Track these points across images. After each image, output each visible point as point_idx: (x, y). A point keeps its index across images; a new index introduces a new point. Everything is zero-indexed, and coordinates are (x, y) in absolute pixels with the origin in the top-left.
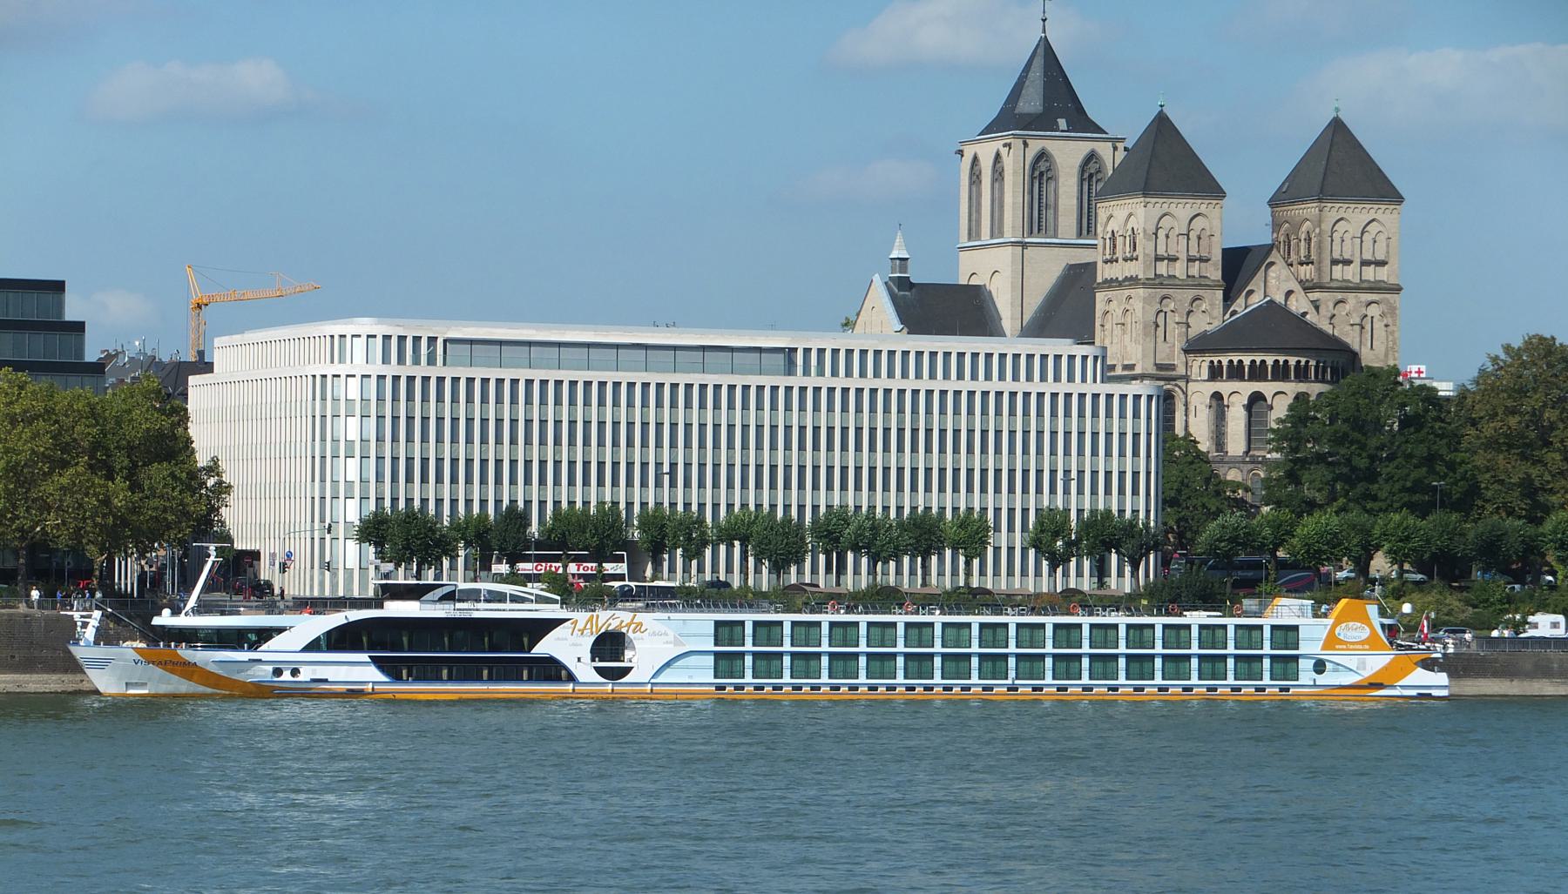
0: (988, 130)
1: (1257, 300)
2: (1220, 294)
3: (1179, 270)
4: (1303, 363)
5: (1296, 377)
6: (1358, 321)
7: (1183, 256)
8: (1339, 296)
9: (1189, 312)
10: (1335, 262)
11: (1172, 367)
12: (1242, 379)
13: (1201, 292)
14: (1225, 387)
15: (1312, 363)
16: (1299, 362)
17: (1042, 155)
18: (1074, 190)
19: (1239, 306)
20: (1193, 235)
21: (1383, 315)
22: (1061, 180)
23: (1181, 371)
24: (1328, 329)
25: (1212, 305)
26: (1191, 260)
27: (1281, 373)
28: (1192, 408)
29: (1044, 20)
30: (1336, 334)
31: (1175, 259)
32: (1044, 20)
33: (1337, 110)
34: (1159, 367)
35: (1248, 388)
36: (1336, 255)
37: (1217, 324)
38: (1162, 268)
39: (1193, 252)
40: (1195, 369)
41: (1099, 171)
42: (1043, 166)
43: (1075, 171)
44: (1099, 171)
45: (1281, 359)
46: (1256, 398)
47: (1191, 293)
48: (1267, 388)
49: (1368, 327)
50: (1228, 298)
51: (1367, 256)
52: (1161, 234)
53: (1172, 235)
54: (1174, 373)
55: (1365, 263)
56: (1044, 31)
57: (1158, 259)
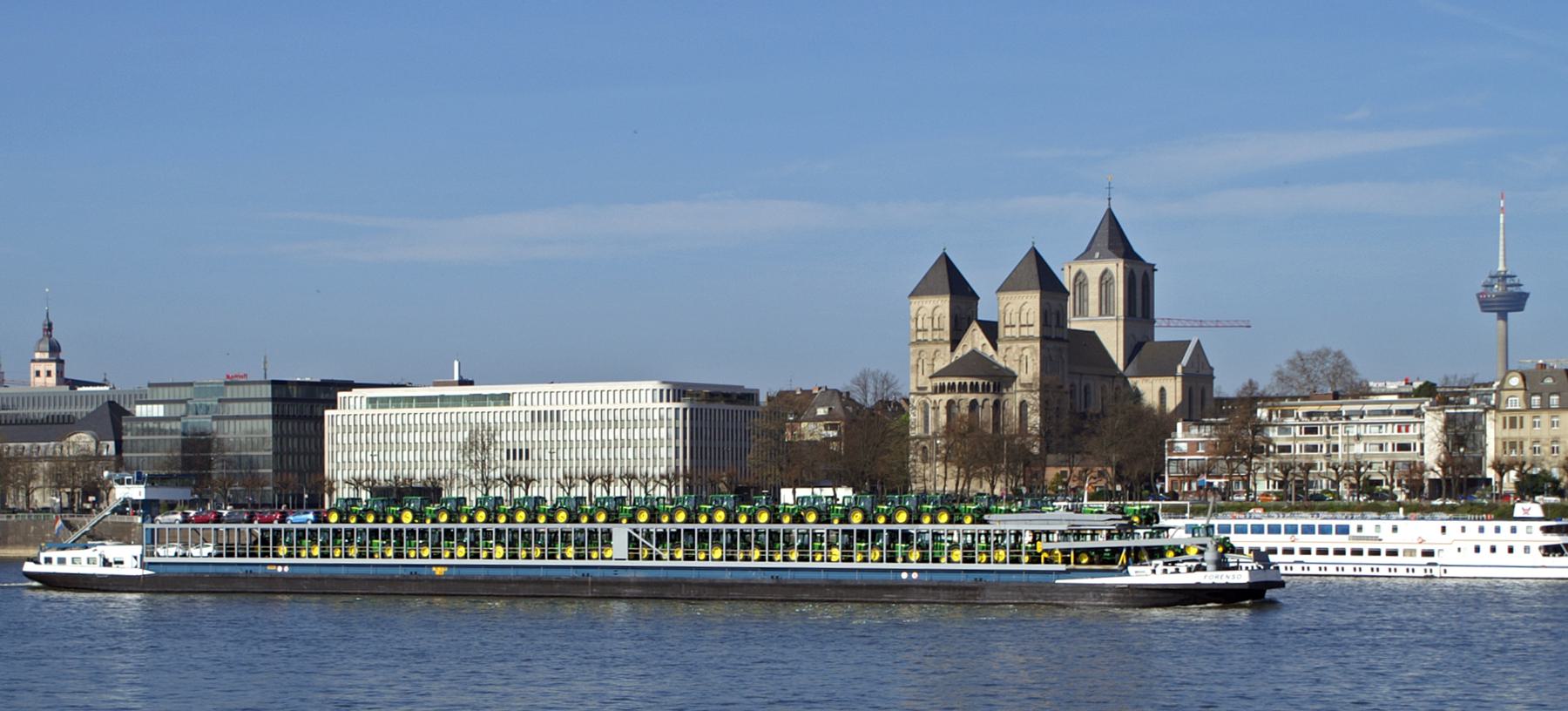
0: (1077, 259)
1: (969, 349)
2: (948, 347)
3: (929, 337)
4: (986, 383)
5: (994, 390)
6: (1017, 358)
7: (930, 329)
8: (1008, 345)
9: (933, 359)
10: (1006, 326)
11: (925, 388)
12: (966, 392)
13: (939, 347)
15: (991, 384)
16: (984, 383)
17: (1079, 273)
18: (1097, 291)
19: (959, 353)
21: (1031, 353)
22: (1090, 286)
24: (1002, 363)
25: (945, 354)
26: (934, 330)
27: (963, 388)
29: (1109, 199)
30: (1008, 366)
31: (926, 330)
32: (1109, 199)
33: (1033, 243)
34: (919, 388)
35: (946, 397)
36: (1008, 323)
37: (947, 364)
38: (920, 336)
39: (936, 326)
41: (1110, 279)
42: (1081, 278)
43: (1097, 280)
44: (1110, 279)
45: (974, 381)
46: (950, 404)
47: (934, 347)
48: (980, 398)
49: (1025, 362)
50: (953, 350)
51: (1024, 322)
52: (920, 319)
53: (925, 318)
54: (926, 392)
55: (1022, 326)
56: (1109, 204)
57: (918, 330)
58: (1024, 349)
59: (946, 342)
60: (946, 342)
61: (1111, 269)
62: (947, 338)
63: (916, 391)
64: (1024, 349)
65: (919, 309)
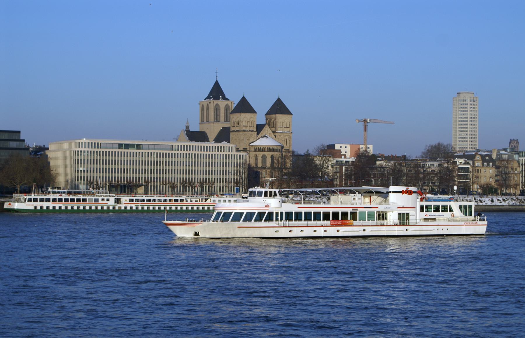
2: (256, 133)
3: (248, 129)
7: (248, 126)
11: (246, 149)
14: (257, 153)
20: (250, 122)
21: (289, 138)
23: (248, 149)
25: (254, 136)
28: (250, 157)
29: (217, 77)
31: (247, 126)
34: (244, 149)
38: (244, 128)
40: (251, 149)
53: (246, 122)
58: (286, 136)
59: (255, 131)
60: (255, 131)
61: (229, 104)
62: (255, 130)
63: (242, 149)
64: (286, 136)
65: (244, 118)
